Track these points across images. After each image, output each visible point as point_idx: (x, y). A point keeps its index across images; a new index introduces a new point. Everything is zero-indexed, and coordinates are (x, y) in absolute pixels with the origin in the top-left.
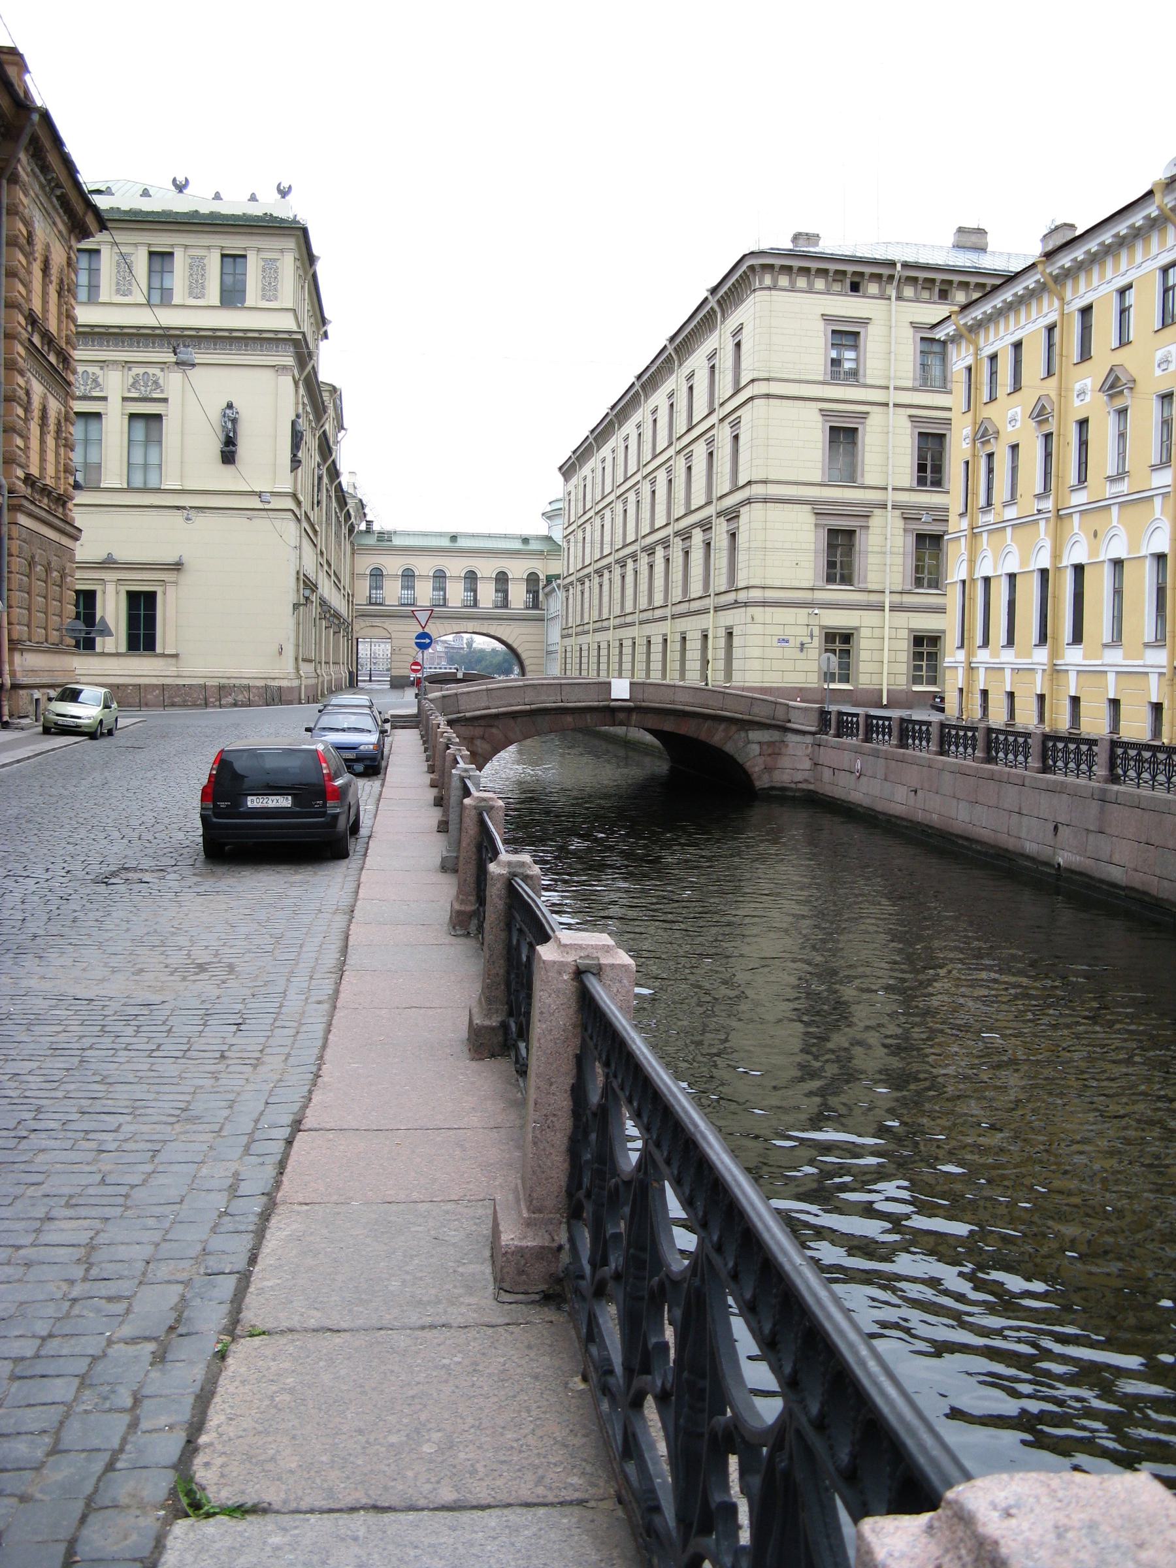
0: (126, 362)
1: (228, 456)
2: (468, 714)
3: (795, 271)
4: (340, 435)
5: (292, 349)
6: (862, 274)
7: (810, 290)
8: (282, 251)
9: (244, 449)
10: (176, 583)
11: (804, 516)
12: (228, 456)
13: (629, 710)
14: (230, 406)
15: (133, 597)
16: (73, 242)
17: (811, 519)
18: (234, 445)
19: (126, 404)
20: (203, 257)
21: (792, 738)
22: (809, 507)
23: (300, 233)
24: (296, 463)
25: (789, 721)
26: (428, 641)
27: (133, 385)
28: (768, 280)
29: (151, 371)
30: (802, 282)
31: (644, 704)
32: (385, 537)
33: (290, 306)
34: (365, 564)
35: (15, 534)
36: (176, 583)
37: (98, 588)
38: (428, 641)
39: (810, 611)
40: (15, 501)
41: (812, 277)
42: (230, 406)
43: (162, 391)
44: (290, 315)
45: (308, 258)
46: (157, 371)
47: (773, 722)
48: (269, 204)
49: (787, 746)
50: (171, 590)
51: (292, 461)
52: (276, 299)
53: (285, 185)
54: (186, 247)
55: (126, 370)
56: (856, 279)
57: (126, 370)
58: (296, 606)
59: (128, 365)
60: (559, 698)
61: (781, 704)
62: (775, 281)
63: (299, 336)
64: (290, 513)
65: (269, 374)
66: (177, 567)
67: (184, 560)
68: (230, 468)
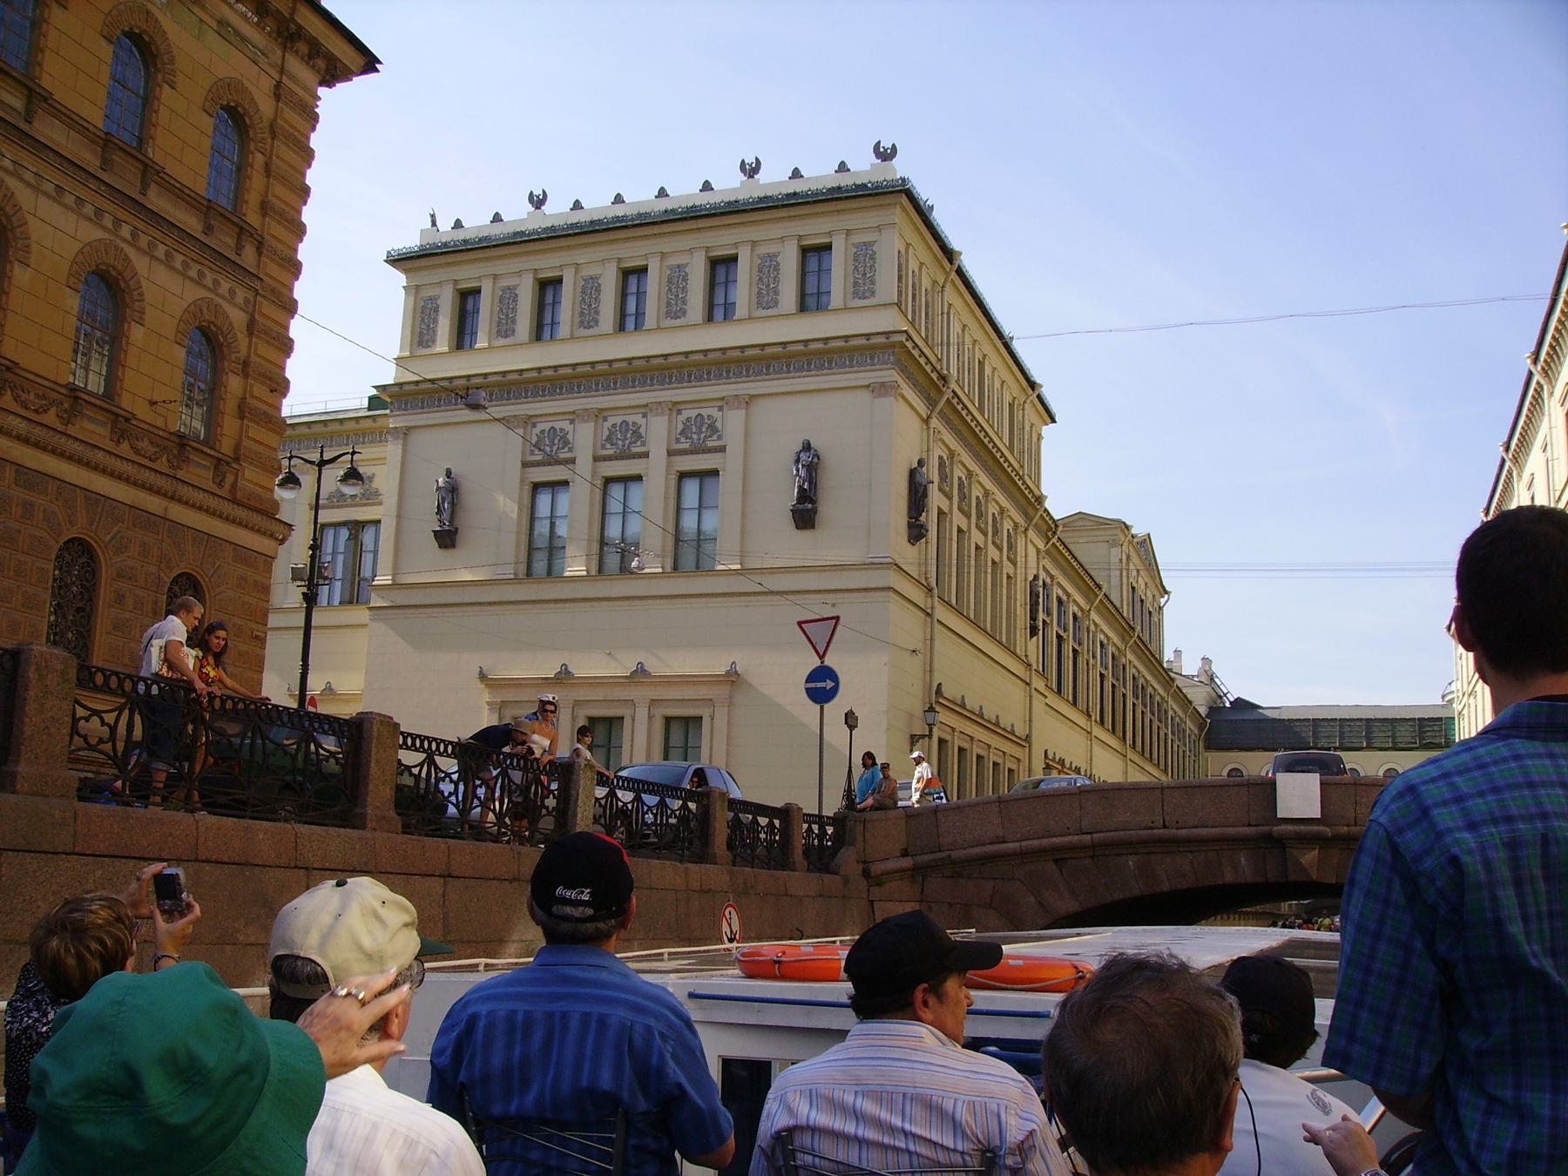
1: (805, 515)
4: (1163, 601)
8: (879, 228)
9: (830, 507)
12: (805, 515)
14: (807, 447)
18: (813, 502)
20: (776, 255)
23: (904, 199)
24: (916, 532)
26: (829, 684)
38: (829, 684)
42: (807, 447)
48: (863, 166)
51: (910, 526)
53: (886, 144)
63: (903, 338)
65: (865, 396)
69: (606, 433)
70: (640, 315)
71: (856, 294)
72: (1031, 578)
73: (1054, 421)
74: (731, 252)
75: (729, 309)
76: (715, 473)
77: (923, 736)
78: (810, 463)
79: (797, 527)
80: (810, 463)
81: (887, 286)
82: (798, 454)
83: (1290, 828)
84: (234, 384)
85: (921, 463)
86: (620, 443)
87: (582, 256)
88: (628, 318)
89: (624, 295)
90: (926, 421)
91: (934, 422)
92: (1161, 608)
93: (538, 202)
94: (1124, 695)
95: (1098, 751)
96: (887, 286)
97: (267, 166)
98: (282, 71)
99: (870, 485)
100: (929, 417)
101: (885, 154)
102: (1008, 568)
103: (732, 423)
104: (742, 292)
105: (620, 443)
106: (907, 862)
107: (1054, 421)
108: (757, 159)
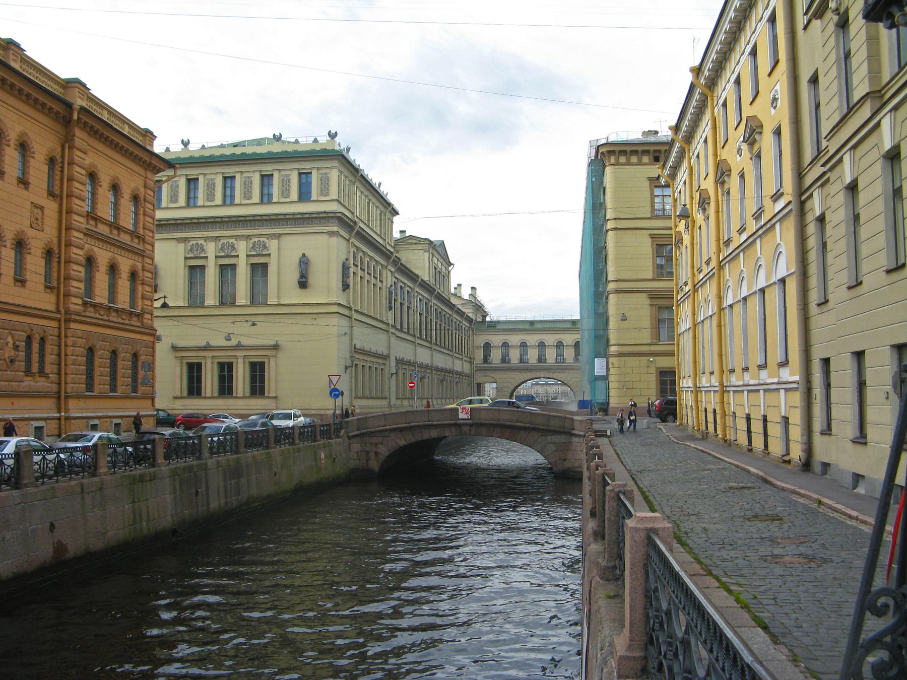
0: (217, 237)
1: (303, 284)
2: (372, 430)
3: (628, 153)
4: (450, 268)
5: (336, 222)
6: (660, 151)
7: (640, 163)
8: (331, 168)
9: (311, 280)
10: (275, 356)
11: (643, 299)
12: (303, 284)
13: (471, 425)
14: (304, 255)
15: (253, 365)
16: (149, 175)
17: (648, 302)
18: (306, 277)
19: (218, 259)
21: (575, 440)
22: (644, 295)
24: (346, 287)
25: (574, 429)
27: (252, 248)
28: (613, 160)
29: (262, 239)
30: (634, 159)
31: (479, 421)
32: (494, 325)
33: (336, 197)
34: (481, 339)
35: (69, 334)
36: (275, 356)
37: (234, 361)
39: (648, 358)
40: (68, 317)
41: (640, 155)
42: (304, 255)
43: (268, 251)
44: (336, 203)
45: (354, 170)
46: (265, 239)
47: (563, 430)
49: (572, 445)
50: (272, 361)
52: (328, 195)
53: (333, 131)
54: (280, 171)
55: (249, 240)
56: (656, 155)
57: (249, 240)
58: (346, 368)
59: (249, 237)
60: (427, 420)
61: (568, 418)
62: (617, 160)
64: (337, 315)
66: (276, 347)
67: (279, 343)
68: (304, 291)
69: (220, 246)
70: (232, 197)
71: (322, 194)
72: (389, 286)
73: (398, 214)
74: (271, 173)
75: (270, 196)
76: (266, 264)
77: (350, 366)
78: (304, 263)
79: (300, 288)
80: (304, 263)
81: (334, 195)
82: (300, 259)
83: (462, 421)
84: (140, 287)
85: (347, 259)
86: (226, 251)
87: (206, 171)
88: (227, 197)
89: (225, 188)
90: (348, 241)
91: (352, 240)
92: (449, 272)
93: (186, 144)
94: (431, 319)
95: (420, 350)
96: (334, 195)
97: (144, 211)
98: (146, 178)
99: (328, 272)
100: (350, 239)
101: (333, 136)
102: (379, 284)
103: (273, 245)
104: (276, 190)
105: (226, 251)
106: (358, 432)
107: (398, 214)
108: (280, 134)
